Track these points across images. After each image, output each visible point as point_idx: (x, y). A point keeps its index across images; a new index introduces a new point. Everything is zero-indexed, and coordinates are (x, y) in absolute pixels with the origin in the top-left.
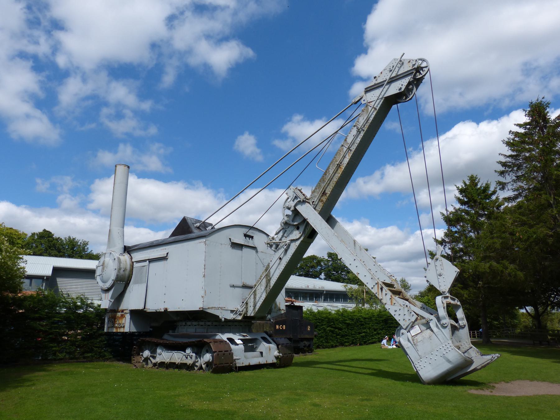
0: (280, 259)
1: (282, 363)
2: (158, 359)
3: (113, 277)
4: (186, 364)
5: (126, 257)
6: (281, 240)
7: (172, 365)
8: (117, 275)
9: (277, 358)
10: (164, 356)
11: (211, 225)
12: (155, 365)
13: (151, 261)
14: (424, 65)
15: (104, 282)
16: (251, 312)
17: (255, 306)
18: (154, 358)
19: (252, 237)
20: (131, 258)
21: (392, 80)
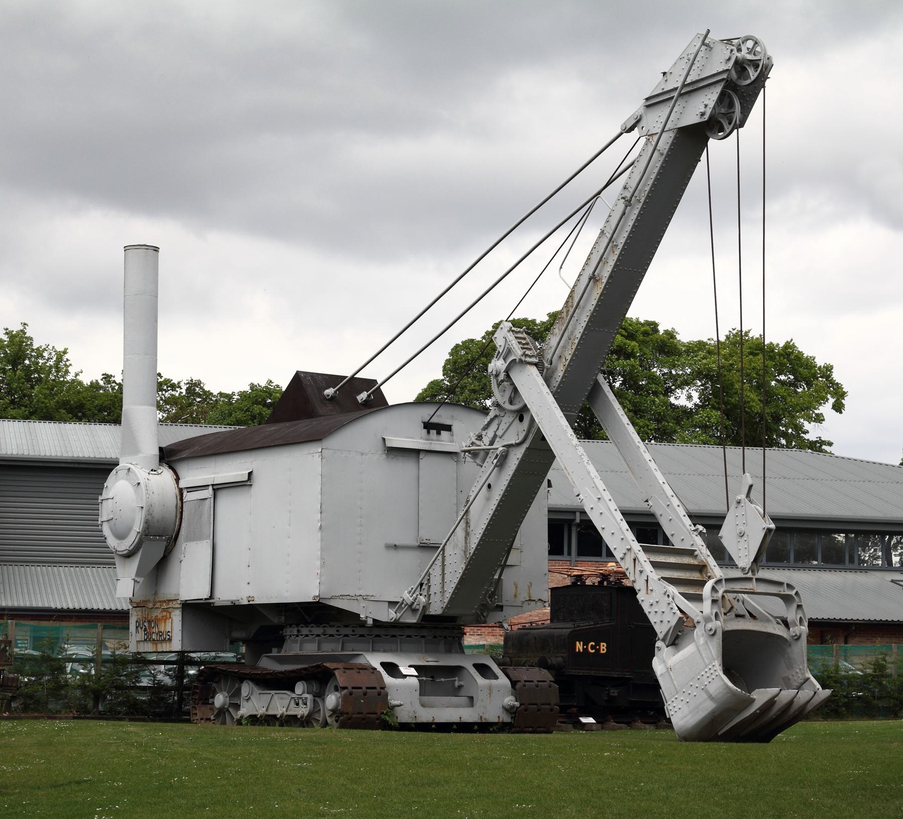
0: (489, 486)
2: (245, 710)
4: (296, 716)
5: (167, 474)
7: (269, 720)
8: (147, 522)
10: (255, 702)
11: (370, 383)
12: (239, 722)
13: (217, 488)
15: (121, 537)
16: (436, 609)
17: (443, 592)
18: (237, 707)
19: (448, 428)
20: (177, 480)
21: (690, 89)
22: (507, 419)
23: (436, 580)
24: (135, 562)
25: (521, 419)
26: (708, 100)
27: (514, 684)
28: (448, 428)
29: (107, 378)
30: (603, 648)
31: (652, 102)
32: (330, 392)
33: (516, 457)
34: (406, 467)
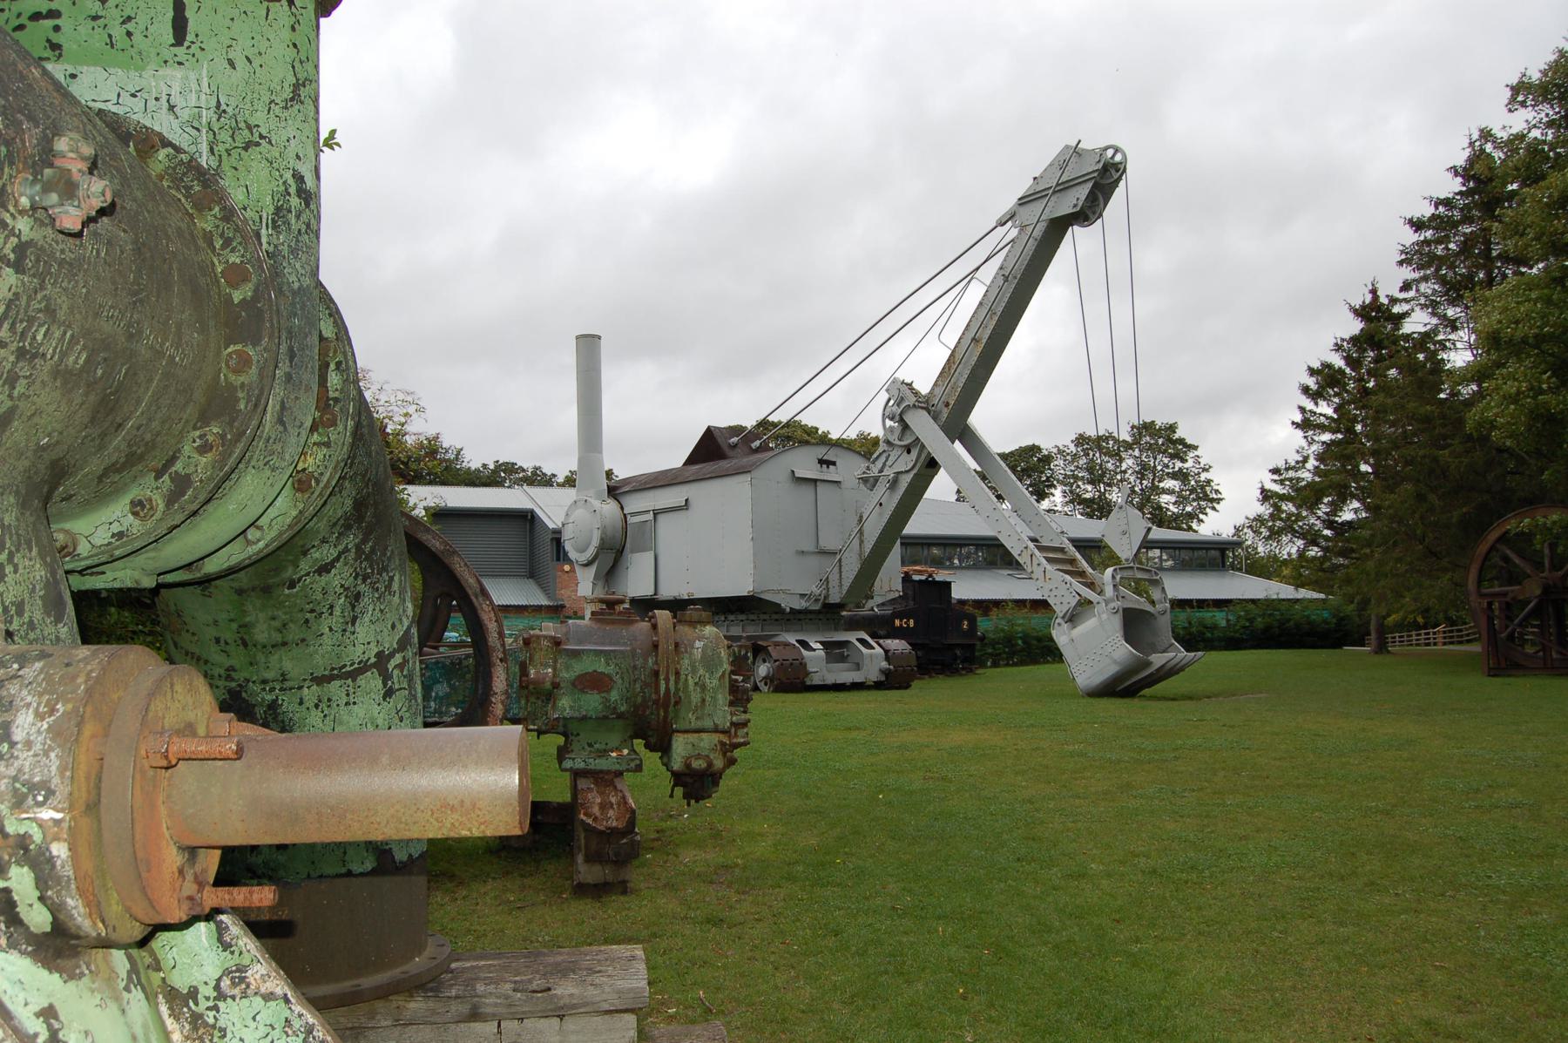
1: (894, 680)
3: (595, 542)
5: (610, 507)
6: (881, 471)
9: (882, 671)
13: (656, 513)
14: (1118, 158)
16: (835, 598)
19: (834, 463)
21: (1063, 188)
22: (894, 454)
23: (834, 578)
24: (593, 569)
25: (909, 452)
26: (1082, 192)
27: (886, 652)
28: (834, 463)
29: (485, 466)
30: (912, 623)
31: (1024, 201)
32: (735, 440)
33: (905, 481)
34: (807, 491)
